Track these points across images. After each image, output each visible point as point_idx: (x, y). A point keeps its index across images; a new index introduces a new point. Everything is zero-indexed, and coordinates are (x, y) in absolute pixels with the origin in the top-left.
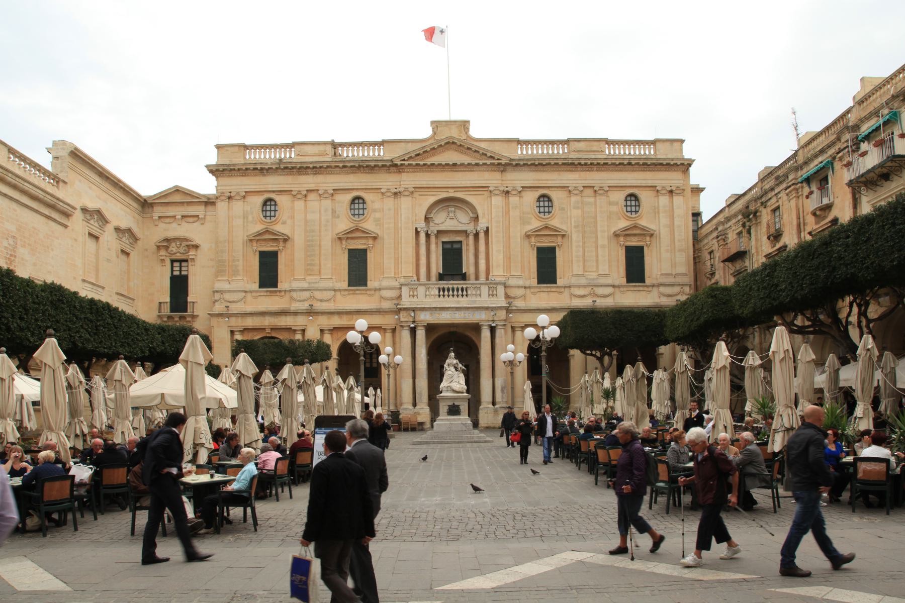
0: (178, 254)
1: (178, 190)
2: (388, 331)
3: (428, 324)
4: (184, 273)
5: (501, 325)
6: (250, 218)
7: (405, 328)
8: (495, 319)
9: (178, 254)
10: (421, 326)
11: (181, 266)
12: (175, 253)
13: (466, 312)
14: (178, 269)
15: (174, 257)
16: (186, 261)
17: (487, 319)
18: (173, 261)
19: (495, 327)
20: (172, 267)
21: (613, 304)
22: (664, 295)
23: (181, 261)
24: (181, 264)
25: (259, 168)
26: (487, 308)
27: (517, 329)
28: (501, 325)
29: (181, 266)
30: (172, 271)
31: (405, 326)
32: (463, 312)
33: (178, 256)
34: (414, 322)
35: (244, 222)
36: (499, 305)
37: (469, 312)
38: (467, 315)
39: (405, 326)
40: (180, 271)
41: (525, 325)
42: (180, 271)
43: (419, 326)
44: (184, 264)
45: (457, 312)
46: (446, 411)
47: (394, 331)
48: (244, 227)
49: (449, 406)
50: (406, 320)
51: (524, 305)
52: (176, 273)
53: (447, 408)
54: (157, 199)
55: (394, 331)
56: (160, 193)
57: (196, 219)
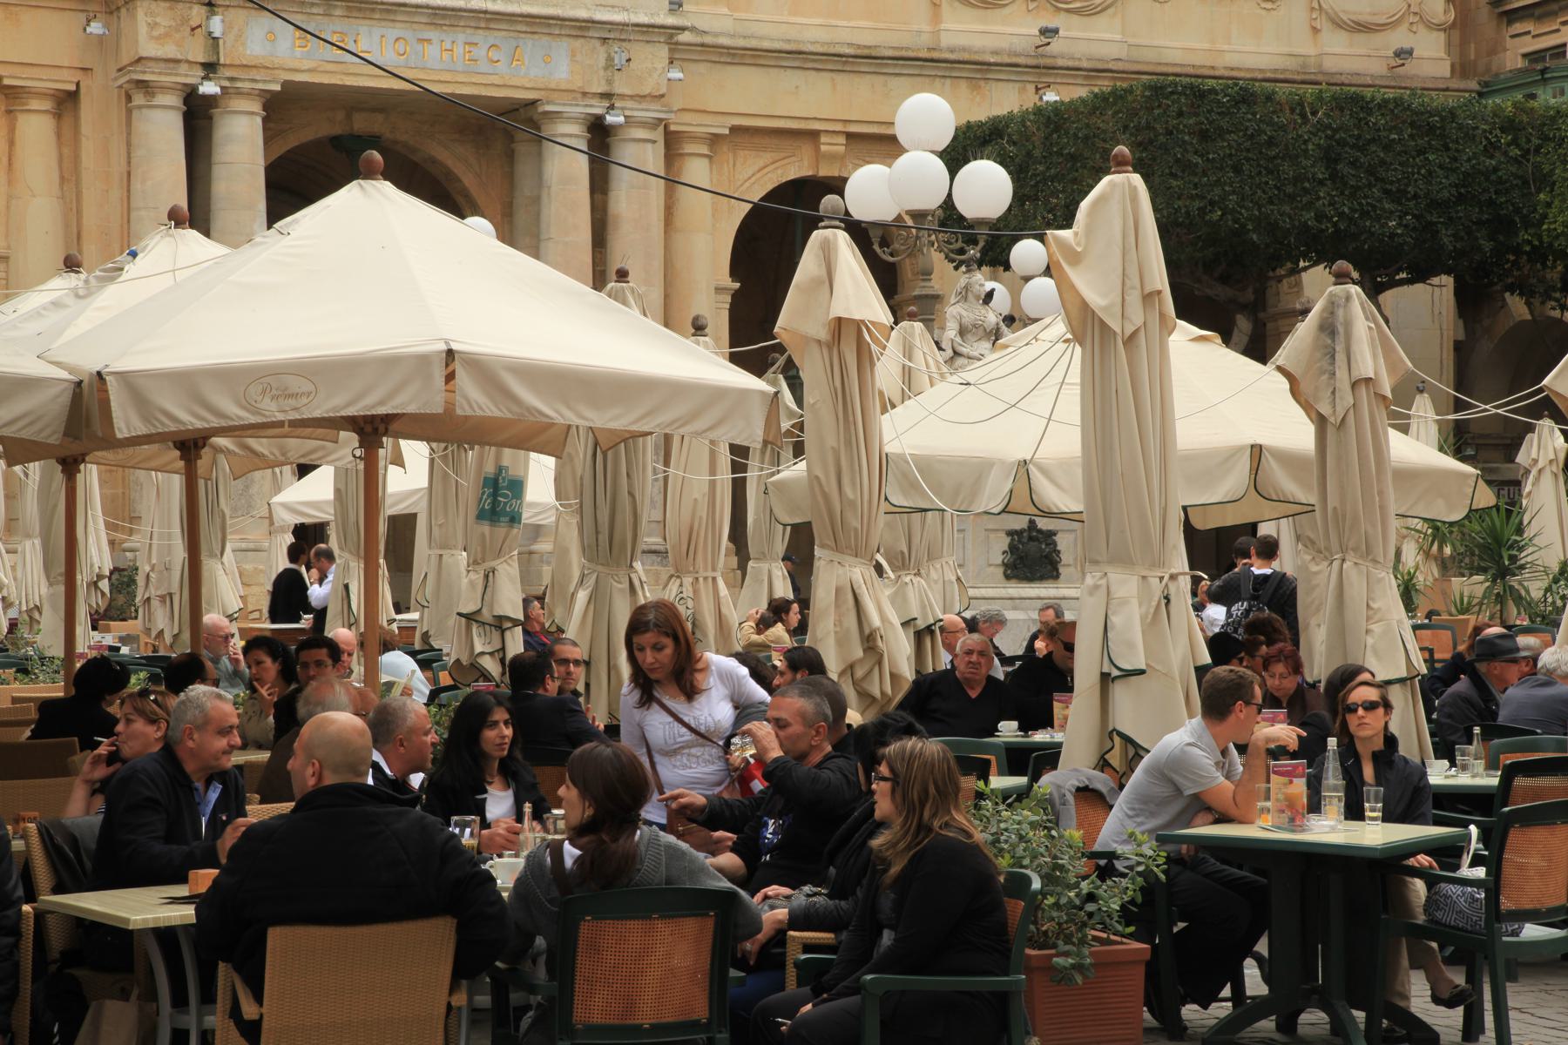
2: (35, 104)
3: (285, 84)
5: (644, 124)
7: (163, 99)
8: (620, 87)
10: (247, 95)
13: (478, 36)
17: (578, 84)
19: (211, 101)
21: (1121, 52)
22: (1338, 24)
26: (582, 28)
27: (689, 148)
28: (644, 124)
31: (164, 88)
32: (461, 37)
34: (210, 68)
36: (635, 19)
37: (492, 38)
38: (481, 52)
39: (164, 88)
41: (735, 130)
43: (240, 93)
45: (432, 34)
46: (999, 559)
47: (67, 102)
49: (1010, 533)
50: (169, 51)
51: (726, 25)
53: (1004, 542)
55: (67, 102)
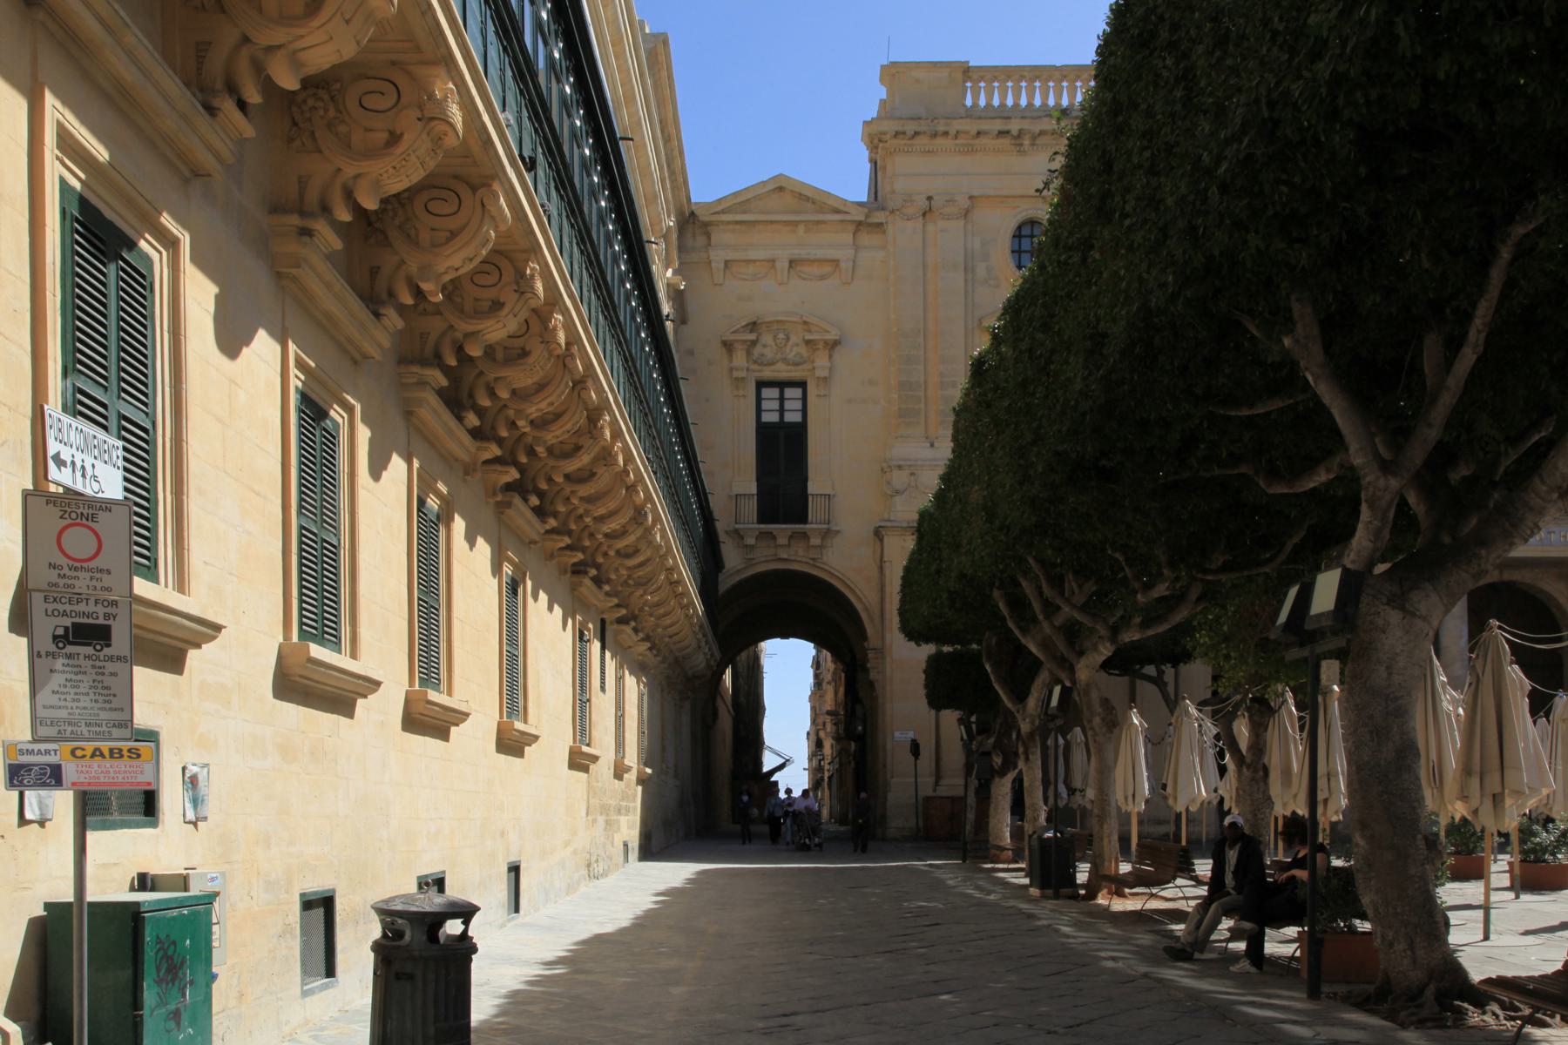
0: (780, 366)
1: (781, 189)
4: (793, 417)
6: (981, 271)
9: (780, 366)
11: (782, 399)
12: (773, 364)
14: (775, 405)
15: (768, 374)
18: (761, 384)
20: (759, 400)
23: (781, 385)
25: (1015, 132)
29: (782, 399)
30: (759, 410)
33: (781, 372)
35: (966, 280)
40: (782, 411)
42: (782, 411)
44: (790, 393)
48: (966, 293)
52: (770, 417)
54: (723, 212)
56: (735, 194)
57: (827, 269)
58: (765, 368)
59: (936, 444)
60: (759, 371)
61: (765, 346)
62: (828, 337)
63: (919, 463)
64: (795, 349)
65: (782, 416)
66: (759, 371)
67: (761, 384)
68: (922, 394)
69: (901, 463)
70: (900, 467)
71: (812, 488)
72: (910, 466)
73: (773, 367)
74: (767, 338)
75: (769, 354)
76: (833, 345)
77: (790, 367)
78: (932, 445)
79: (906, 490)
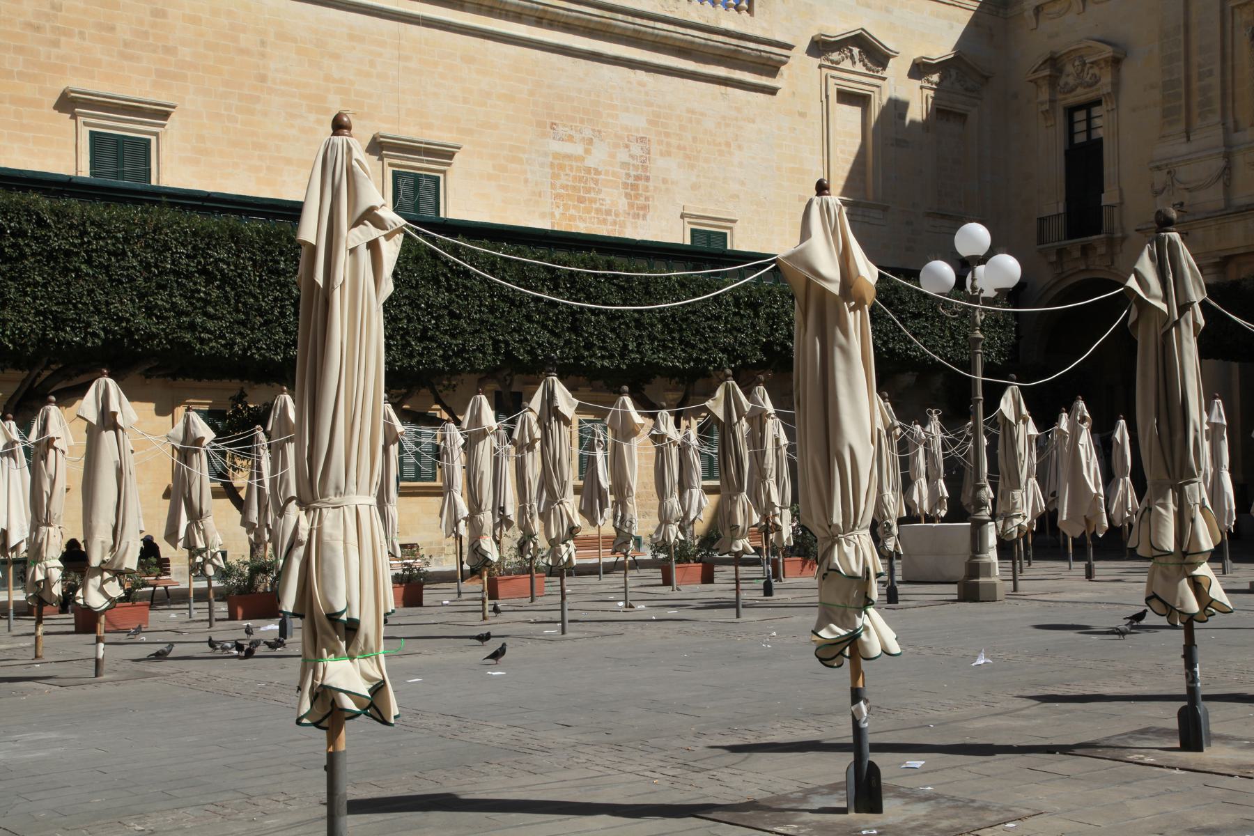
0: (1080, 90)
12: (1072, 90)
15: (1072, 99)
16: (1098, 102)
20: (1071, 123)
24: (1089, 114)
29: (1089, 119)
30: (1071, 133)
33: (1081, 95)
58: (1068, 95)
59: (1192, 138)
60: (1065, 99)
61: (1068, 75)
62: (1105, 55)
63: (1174, 160)
64: (1091, 71)
65: (1089, 135)
66: (1065, 99)
67: (1071, 111)
68: (1182, 90)
69: (1158, 164)
70: (1159, 168)
71: (1107, 198)
72: (1167, 165)
73: (1073, 94)
74: (1069, 68)
75: (1071, 81)
76: (1116, 62)
77: (1087, 90)
78: (1188, 139)
79: (1164, 189)
